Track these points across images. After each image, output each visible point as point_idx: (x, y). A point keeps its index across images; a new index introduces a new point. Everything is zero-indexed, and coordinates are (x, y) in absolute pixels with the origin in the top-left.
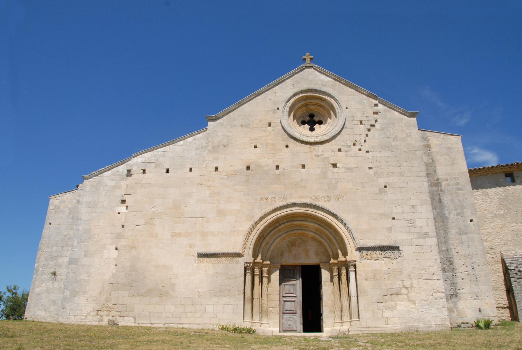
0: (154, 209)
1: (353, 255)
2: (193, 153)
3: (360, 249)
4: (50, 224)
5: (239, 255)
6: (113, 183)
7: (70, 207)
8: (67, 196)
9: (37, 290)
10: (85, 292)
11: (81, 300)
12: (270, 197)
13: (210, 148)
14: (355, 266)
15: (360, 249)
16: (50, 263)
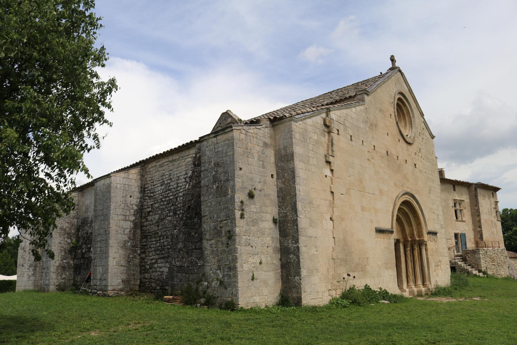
0: (349, 179)
1: (426, 237)
2: (362, 125)
3: (429, 233)
4: (241, 169)
5: (392, 232)
6: (315, 137)
7: (258, 150)
8: (252, 131)
9: (246, 267)
10: (317, 270)
11: (315, 279)
12: (398, 183)
13: (369, 124)
14: (426, 245)
15: (429, 233)
16: (252, 228)
